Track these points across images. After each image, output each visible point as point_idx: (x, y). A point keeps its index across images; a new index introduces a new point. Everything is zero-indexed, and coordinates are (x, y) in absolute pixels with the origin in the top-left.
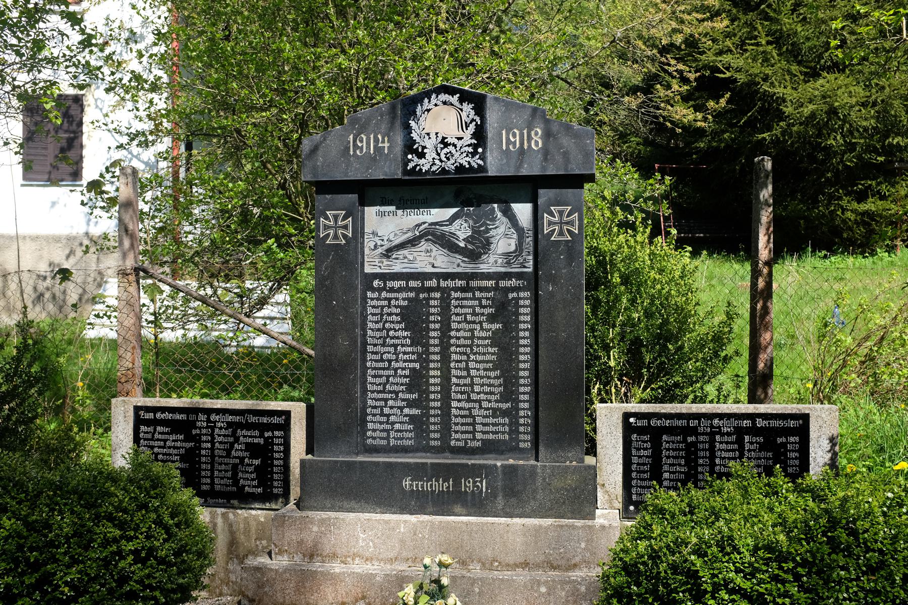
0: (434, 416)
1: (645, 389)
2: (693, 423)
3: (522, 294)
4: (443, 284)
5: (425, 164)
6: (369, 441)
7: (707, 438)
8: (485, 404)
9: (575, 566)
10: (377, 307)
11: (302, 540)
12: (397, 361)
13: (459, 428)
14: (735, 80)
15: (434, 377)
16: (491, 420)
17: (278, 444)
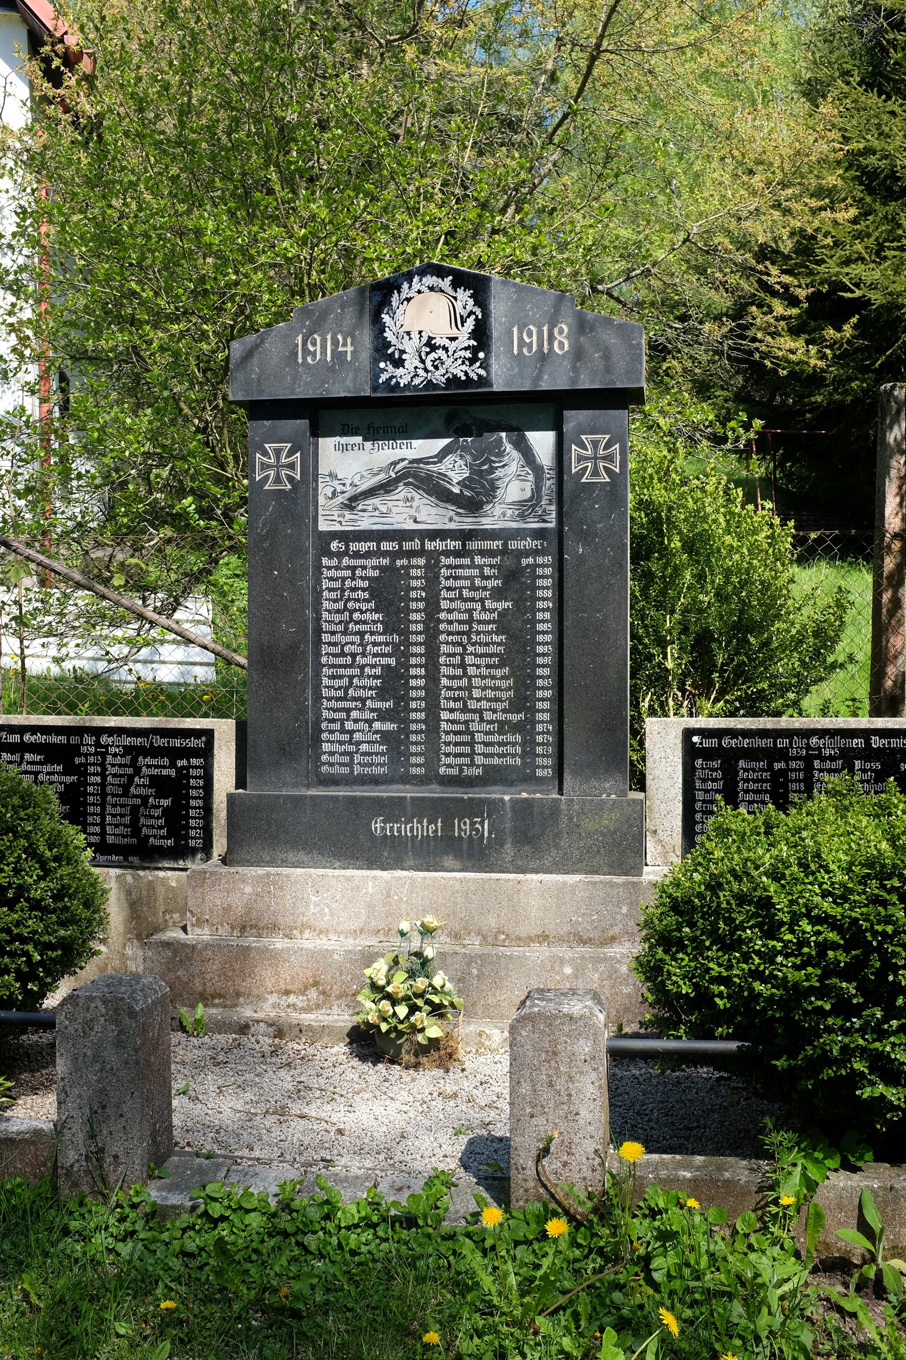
0: (416, 732)
1: (714, 703)
2: (782, 743)
3: (540, 560)
4: (429, 545)
5: (403, 376)
6: (324, 769)
7: (801, 764)
8: (488, 716)
9: (613, 938)
10: (337, 579)
11: (230, 906)
12: (364, 654)
13: (450, 749)
14: (869, 303)
15: (416, 677)
16: (496, 738)
17: (196, 777)
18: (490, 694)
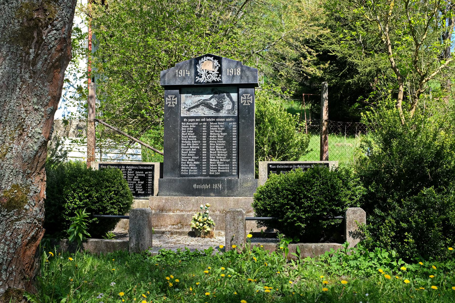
3: (234, 123)
4: (207, 120)
5: (202, 80)
6: (182, 173)
8: (221, 160)
12: (192, 146)
14: (337, 56)
18: (222, 155)
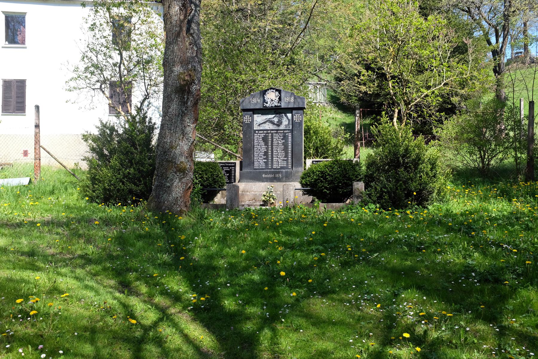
5: (268, 105)
